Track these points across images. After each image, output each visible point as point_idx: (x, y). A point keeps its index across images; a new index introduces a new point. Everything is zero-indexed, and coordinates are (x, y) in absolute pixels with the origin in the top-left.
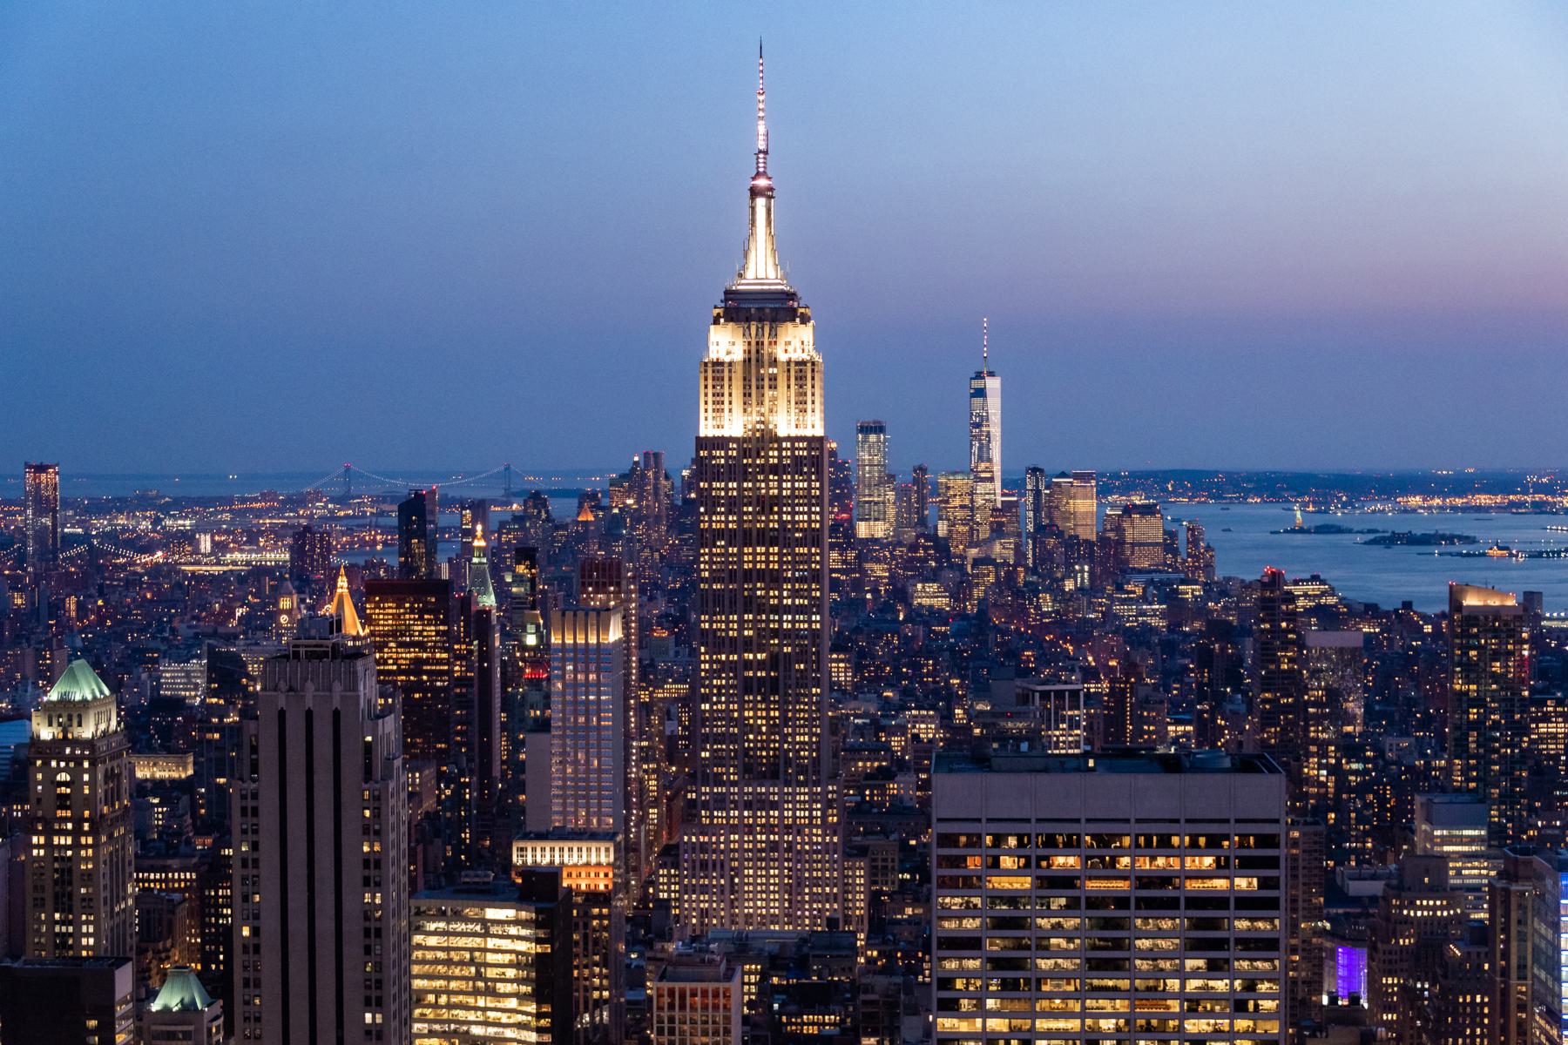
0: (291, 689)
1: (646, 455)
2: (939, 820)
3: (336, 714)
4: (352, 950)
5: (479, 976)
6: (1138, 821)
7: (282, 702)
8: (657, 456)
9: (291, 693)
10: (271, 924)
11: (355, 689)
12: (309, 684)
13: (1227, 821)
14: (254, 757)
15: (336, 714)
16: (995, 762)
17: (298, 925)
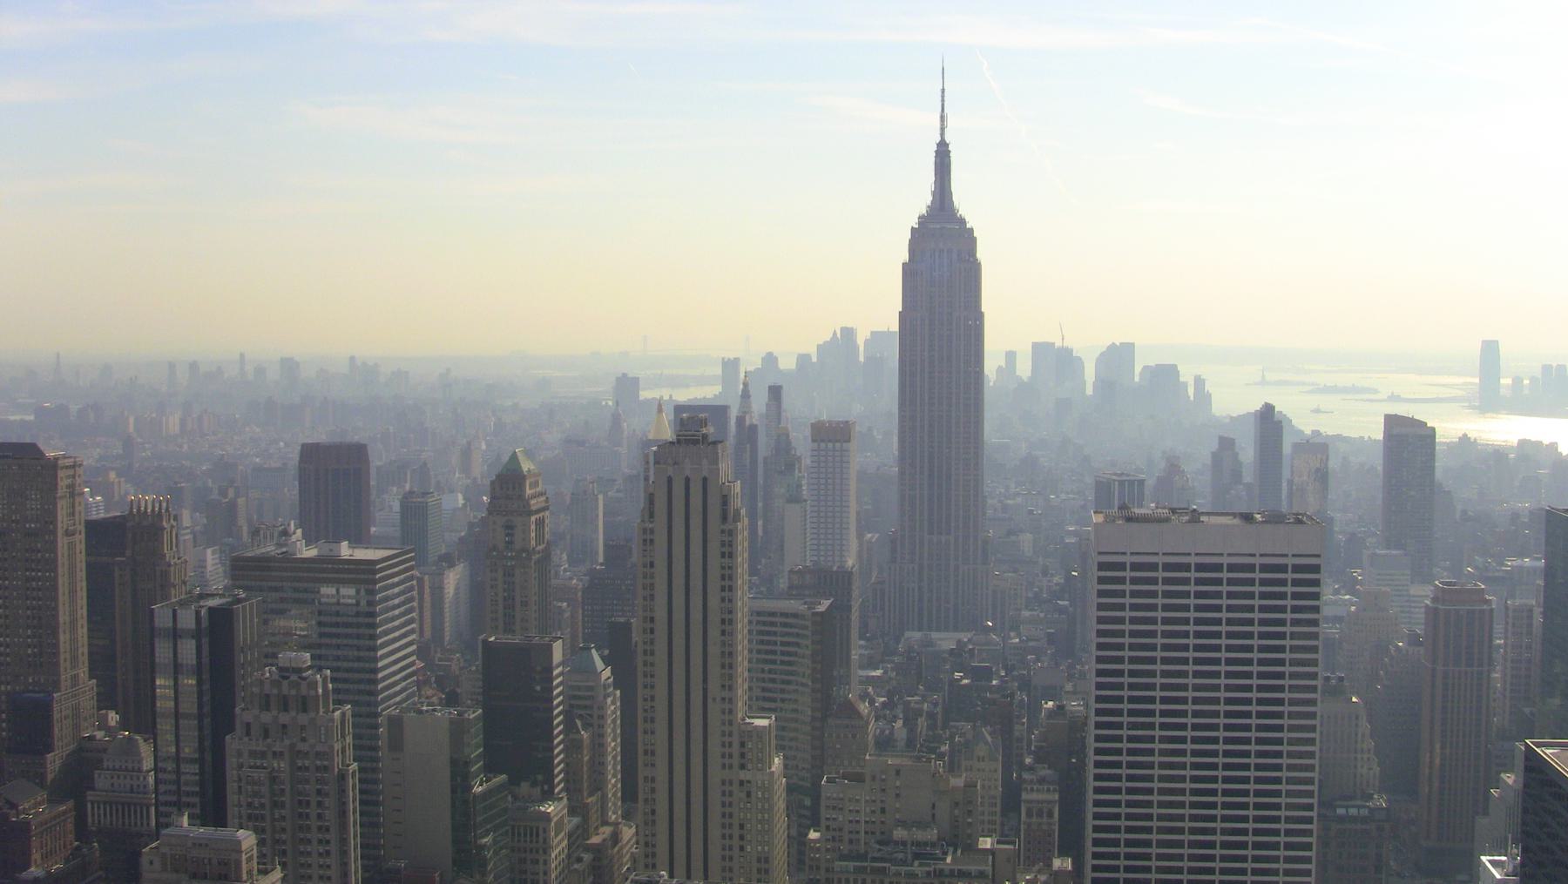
0: (675, 463)
2: (1100, 553)
3: (705, 480)
4: (714, 633)
6: (1229, 555)
9: (676, 466)
10: (661, 614)
11: (717, 464)
13: (1286, 556)
17: (679, 616)
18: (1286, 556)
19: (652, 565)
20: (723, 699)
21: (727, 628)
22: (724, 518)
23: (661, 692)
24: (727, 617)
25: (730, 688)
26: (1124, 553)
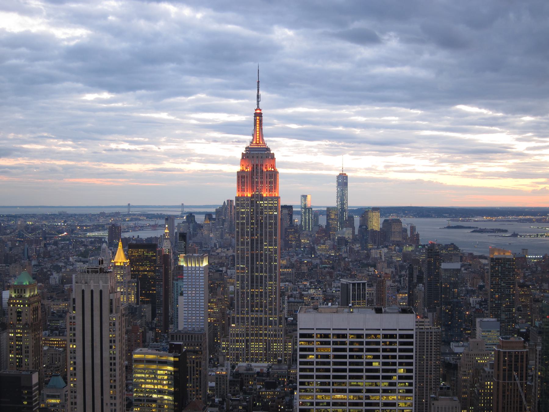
0: (86, 283)
1: (228, 201)
2: (300, 329)
3: (101, 291)
4: (106, 370)
5: (155, 378)
6: (366, 329)
7: (83, 288)
8: (231, 201)
10: (79, 360)
11: (106, 283)
12: (92, 281)
13: (396, 330)
14: (74, 305)
15: (101, 291)
16: (320, 310)
17: (88, 361)
18: (396, 330)
19: (74, 335)
20: (111, 404)
21: (113, 367)
22: (111, 311)
23: (80, 400)
24: (113, 361)
25: (115, 398)
26: (313, 329)
